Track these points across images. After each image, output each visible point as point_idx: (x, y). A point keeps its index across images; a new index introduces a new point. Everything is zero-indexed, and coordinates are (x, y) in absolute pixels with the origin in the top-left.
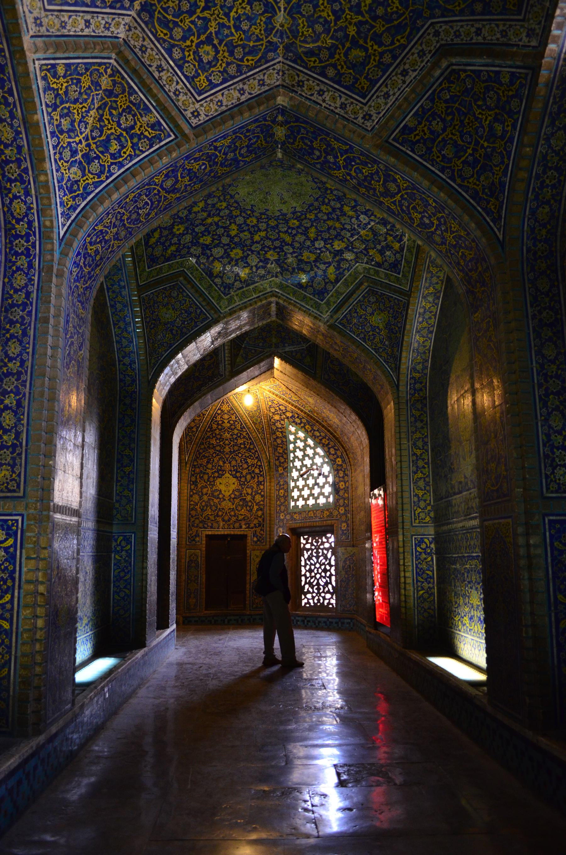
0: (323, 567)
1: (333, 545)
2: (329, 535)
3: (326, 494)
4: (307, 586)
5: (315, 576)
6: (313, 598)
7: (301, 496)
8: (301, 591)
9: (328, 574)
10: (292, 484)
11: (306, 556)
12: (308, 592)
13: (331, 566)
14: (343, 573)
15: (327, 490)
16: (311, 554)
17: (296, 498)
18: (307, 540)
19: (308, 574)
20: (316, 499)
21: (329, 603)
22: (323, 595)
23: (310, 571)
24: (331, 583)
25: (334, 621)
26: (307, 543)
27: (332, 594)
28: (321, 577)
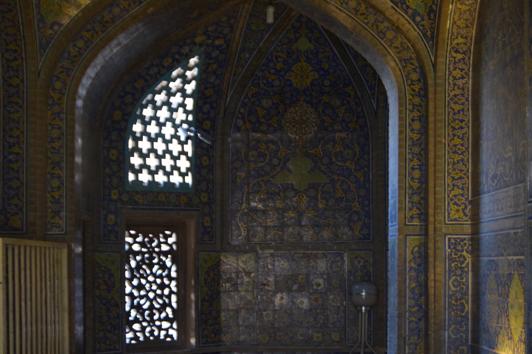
0: (159, 281)
1: (174, 247)
2: (168, 232)
4: (133, 313)
5: (146, 296)
6: (143, 329)
7: (144, 166)
9: (166, 291)
10: (131, 144)
11: (133, 264)
13: (170, 279)
15: (184, 164)
16: (143, 261)
18: (135, 237)
21: (167, 336)
22: (157, 323)
28: (157, 295)
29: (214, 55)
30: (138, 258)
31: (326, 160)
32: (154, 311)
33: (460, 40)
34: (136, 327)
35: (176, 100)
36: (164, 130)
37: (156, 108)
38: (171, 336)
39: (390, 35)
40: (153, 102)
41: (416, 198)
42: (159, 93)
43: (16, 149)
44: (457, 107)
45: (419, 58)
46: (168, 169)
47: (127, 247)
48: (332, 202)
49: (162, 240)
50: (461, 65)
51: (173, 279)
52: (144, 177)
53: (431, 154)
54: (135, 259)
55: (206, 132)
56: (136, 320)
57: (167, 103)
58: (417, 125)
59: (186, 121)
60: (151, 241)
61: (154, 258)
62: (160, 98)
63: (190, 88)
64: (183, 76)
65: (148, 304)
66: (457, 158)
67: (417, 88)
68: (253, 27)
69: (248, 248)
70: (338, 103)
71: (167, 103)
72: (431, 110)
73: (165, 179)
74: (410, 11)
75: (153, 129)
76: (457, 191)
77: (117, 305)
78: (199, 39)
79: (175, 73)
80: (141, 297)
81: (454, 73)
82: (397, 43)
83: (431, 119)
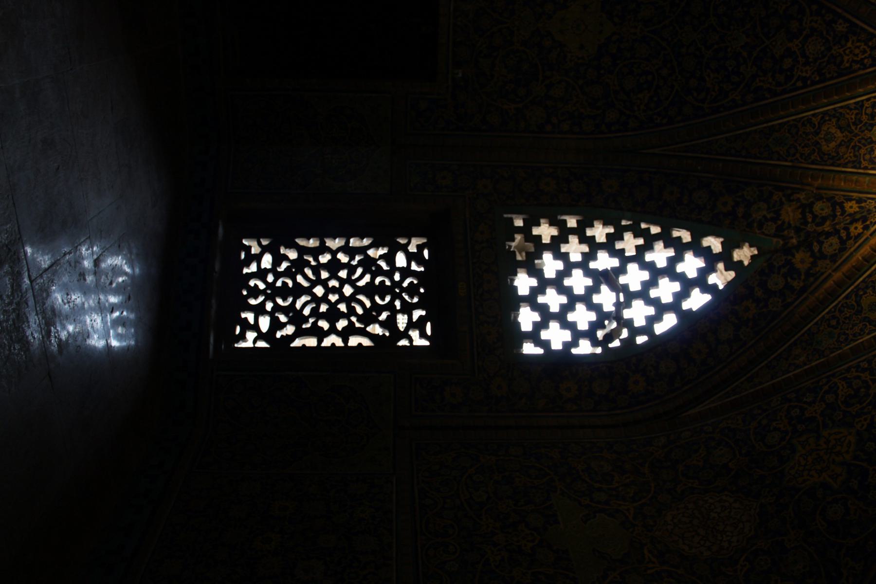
1: (404, 342)
3: (544, 335)
4: (293, 255)
5: (319, 281)
6: (261, 274)
12: (278, 259)
13: (345, 334)
15: (556, 336)
19: (325, 259)
20: (531, 300)
21: (246, 326)
22: (269, 306)
23: (334, 266)
24: (300, 333)
26: (410, 257)
27: (268, 336)
32: (290, 300)
34: (267, 261)
38: (242, 337)
47: (402, 241)
51: (345, 341)
54: (381, 257)
61: (383, 299)
65: (305, 284)
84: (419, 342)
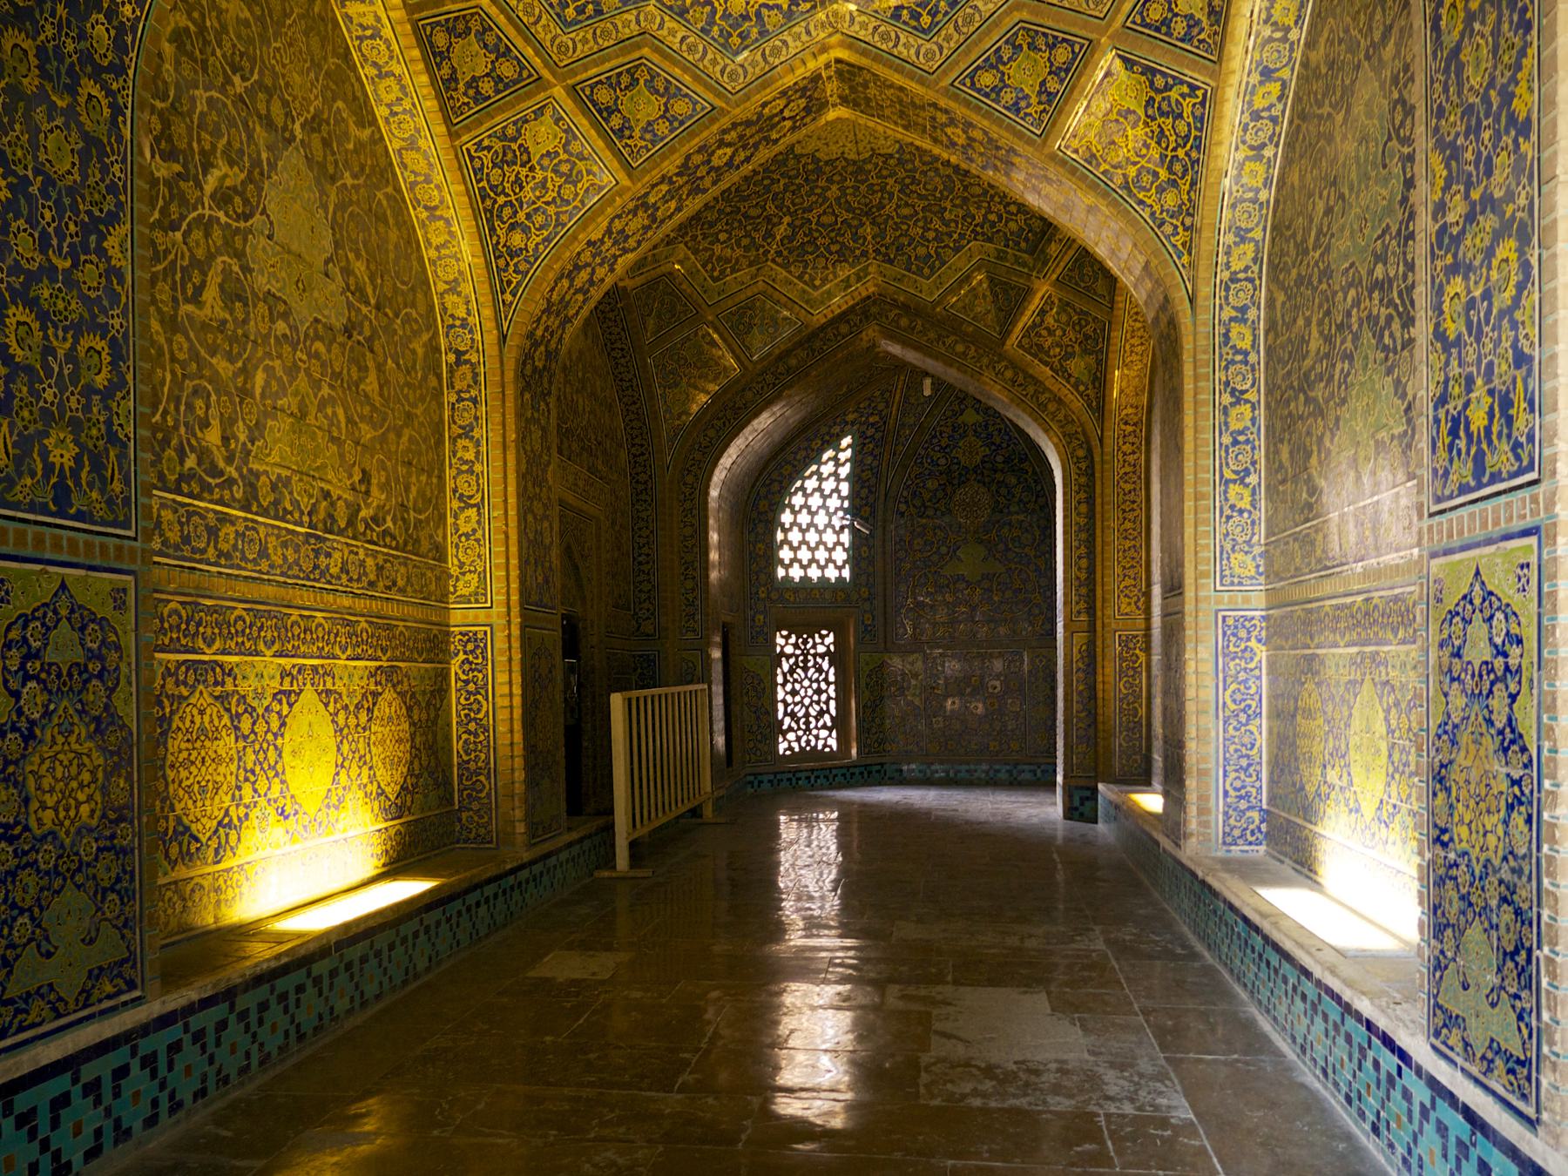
0: (815, 686)
2: (824, 632)
4: (787, 720)
6: (798, 739)
7: (794, 560)
8: (778, 730)
10: (780, 536)
11: (786, 667)
14: (867, 693)
15: (840, 556)
16: (796, 663)
17: (787, 562)
18: (787, 638)
21: (825, 746)
22: (815, 732)
23: (794, 693)
24: (828, 711)
25: (857, 771)
29: (869, 433)
30: (792, 661)
31: (1001, 547)
33: (1130, 411)
35: (829, 485)
36: (817, 520)
37: (806, 495)
39: (1052, 407)
40: (802, 488)
41: (1084, 591)
42: (810, 477)
43: (645, 550)
44: (1128, 487)
45: (1084, 433)
46: (822, 563)
48: (1009, 594)
49: (818, 640)
50: (1131, 439)
52: (796, 573)
53: (1098, 540)
55: (865, 520)
56: (790, 729)
57: (819, 489)
58: (1083, 508)
59: (841, 508)
60: (805, 642)
62: (811, 484)
63: (844, 471)
64: (835, 459)
66: (1128, 544)
67: (1083, 466)
68: (912, 400)
69: (916, 645)
70: (1014, 481)
71: (819, 489)
72: (1098, 491)
73: (819, 573)
74: (1072, 380)
75: (804, 518)
76: (1128, 582)
77: (767, 713)
78: (850, 417)
79: (825, 457)
80: (796, 704)
81: (1124, 448)
82: (1061, 417)
83: (1098, 501)
84: (830, 639)
